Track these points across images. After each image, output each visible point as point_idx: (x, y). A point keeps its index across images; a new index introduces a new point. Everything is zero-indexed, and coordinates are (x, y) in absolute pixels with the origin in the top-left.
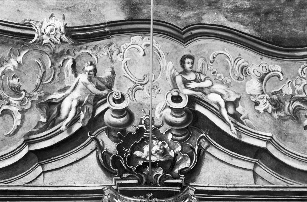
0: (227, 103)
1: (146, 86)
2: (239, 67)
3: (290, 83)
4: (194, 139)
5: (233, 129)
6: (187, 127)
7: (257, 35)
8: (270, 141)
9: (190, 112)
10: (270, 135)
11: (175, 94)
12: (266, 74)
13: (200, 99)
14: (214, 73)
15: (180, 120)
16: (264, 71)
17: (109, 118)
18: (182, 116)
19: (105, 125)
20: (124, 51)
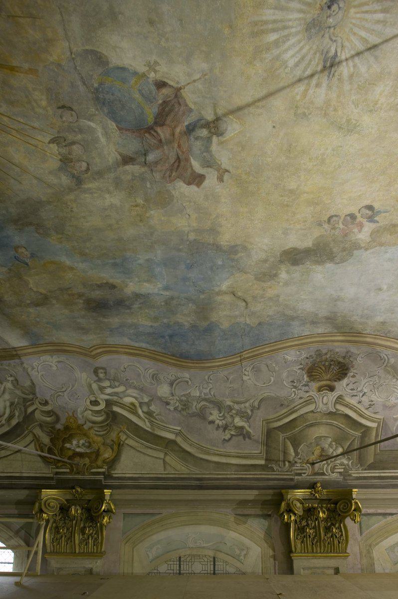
0: (141, 404)
1: (65, 393)
2: (150, 375)
3: (198, 387)
4: (114, 433)
5: (148, 424)
6: (107, 425)
7: (164, 351)
8: (178, 434)
9: (109, 412)
10: (179, 428)
11: (93, 399)
12: (176, 380)
13: (116, 402)
14: (126, 380)
15: (100, 419)
16: (173, 378)
17: (37, 415)
18: (102, 416)
19: (37, 422)
20: (38, 368)
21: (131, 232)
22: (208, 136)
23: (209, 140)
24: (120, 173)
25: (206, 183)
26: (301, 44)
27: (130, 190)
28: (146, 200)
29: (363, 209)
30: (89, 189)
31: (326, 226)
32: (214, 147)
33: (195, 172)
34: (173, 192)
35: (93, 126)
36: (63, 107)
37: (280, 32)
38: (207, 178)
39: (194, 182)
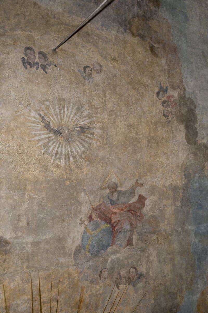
21: (176, 245)
22: (117, 192)
23: (119, 192)
24: (137, 247)
25: (144, 194)
26: (75, 145)
27: (148, 242)
28: (154, 233)
29: (159, 98)
30: (147, 269)
31: (170, 118)
32: (123, 189)
33: (137, 201)
34: (149, 215)
35: (111, 260)
36: (100, 276)
37: (70, 156)
38: (141, 194)
39: (143, 202)
